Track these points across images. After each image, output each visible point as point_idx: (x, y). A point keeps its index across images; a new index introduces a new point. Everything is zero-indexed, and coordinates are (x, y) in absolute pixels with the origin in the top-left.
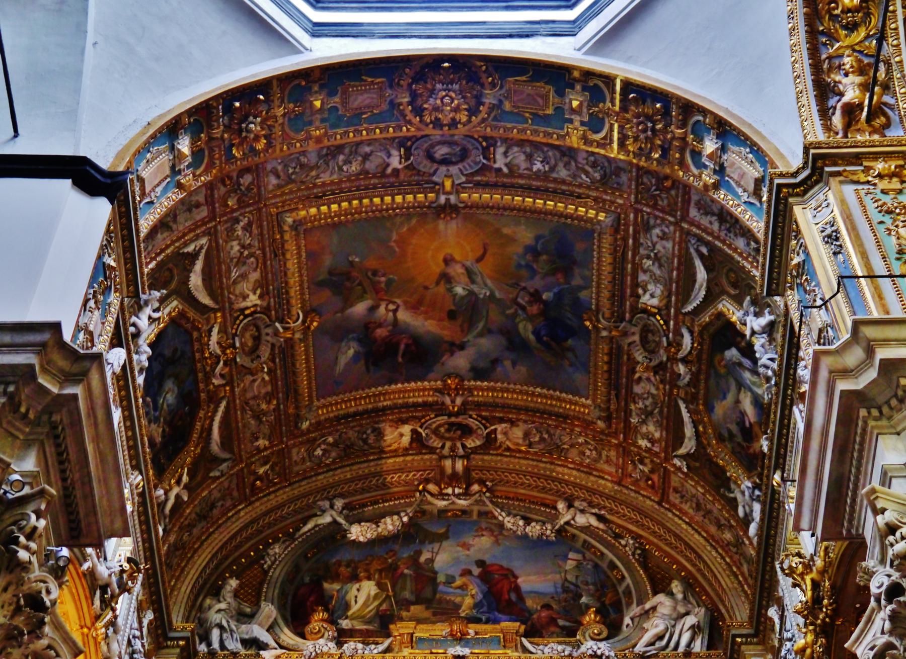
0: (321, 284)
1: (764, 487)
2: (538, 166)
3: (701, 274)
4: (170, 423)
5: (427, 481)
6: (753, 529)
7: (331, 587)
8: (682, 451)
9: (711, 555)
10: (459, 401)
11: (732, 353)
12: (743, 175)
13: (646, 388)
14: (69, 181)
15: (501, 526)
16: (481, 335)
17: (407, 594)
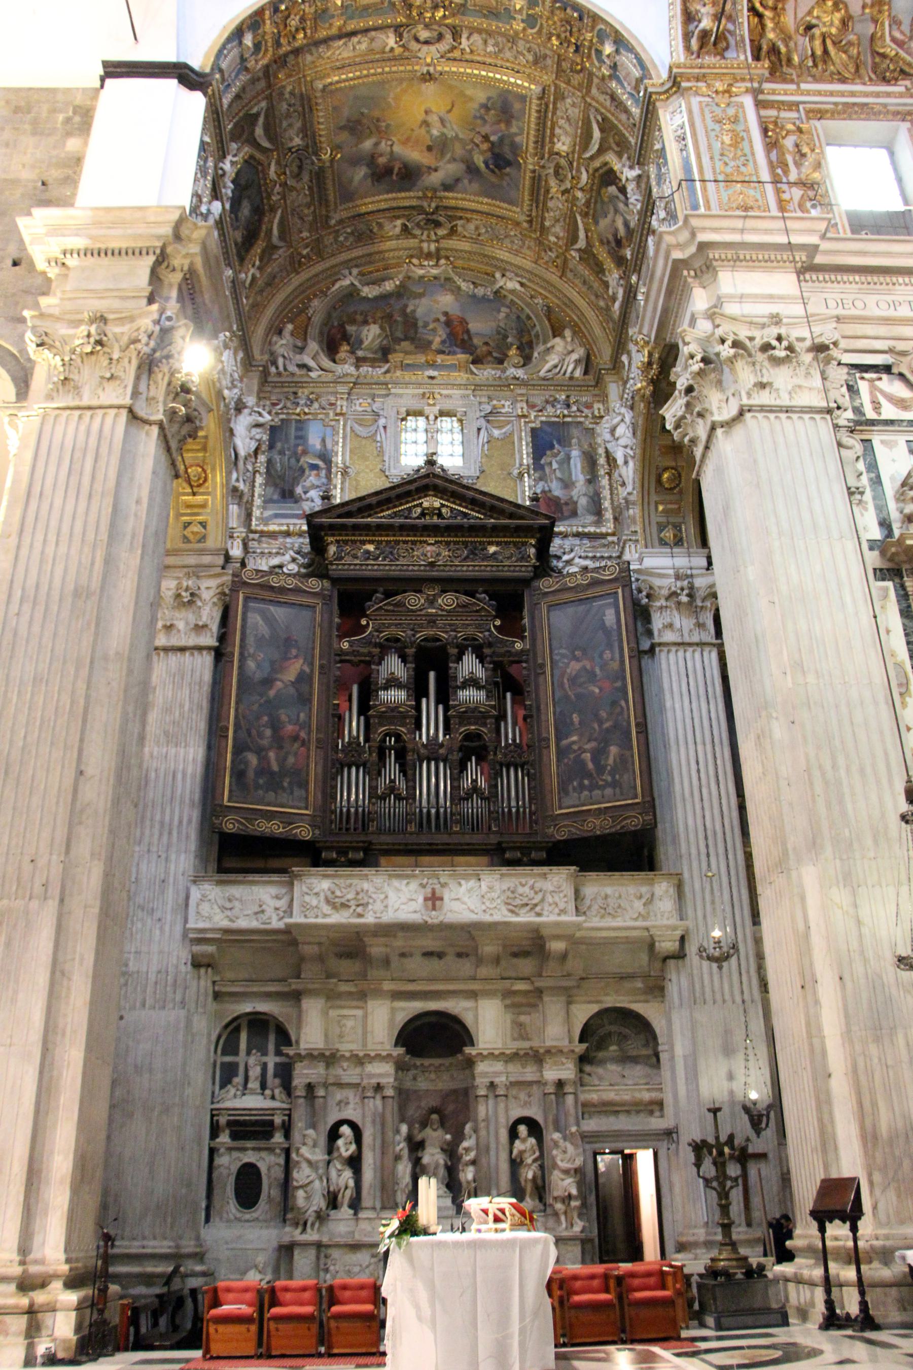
0: (342, 128)
1: (626, 277)
2: (490, 49)
3: (597, 134)
4: (247, 228)
5: (412, 257)
6: (617, 305)
7: (351, 329)
8: (577, 246)
9: (590, 314)
10: (433, 205)
11: (612, 189)
12: (628, 74)
13: (557, 204)
14: (175, 81)
15: (459, 288)
16: (449, 162)
17: (399, 334)
